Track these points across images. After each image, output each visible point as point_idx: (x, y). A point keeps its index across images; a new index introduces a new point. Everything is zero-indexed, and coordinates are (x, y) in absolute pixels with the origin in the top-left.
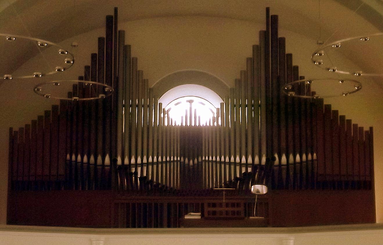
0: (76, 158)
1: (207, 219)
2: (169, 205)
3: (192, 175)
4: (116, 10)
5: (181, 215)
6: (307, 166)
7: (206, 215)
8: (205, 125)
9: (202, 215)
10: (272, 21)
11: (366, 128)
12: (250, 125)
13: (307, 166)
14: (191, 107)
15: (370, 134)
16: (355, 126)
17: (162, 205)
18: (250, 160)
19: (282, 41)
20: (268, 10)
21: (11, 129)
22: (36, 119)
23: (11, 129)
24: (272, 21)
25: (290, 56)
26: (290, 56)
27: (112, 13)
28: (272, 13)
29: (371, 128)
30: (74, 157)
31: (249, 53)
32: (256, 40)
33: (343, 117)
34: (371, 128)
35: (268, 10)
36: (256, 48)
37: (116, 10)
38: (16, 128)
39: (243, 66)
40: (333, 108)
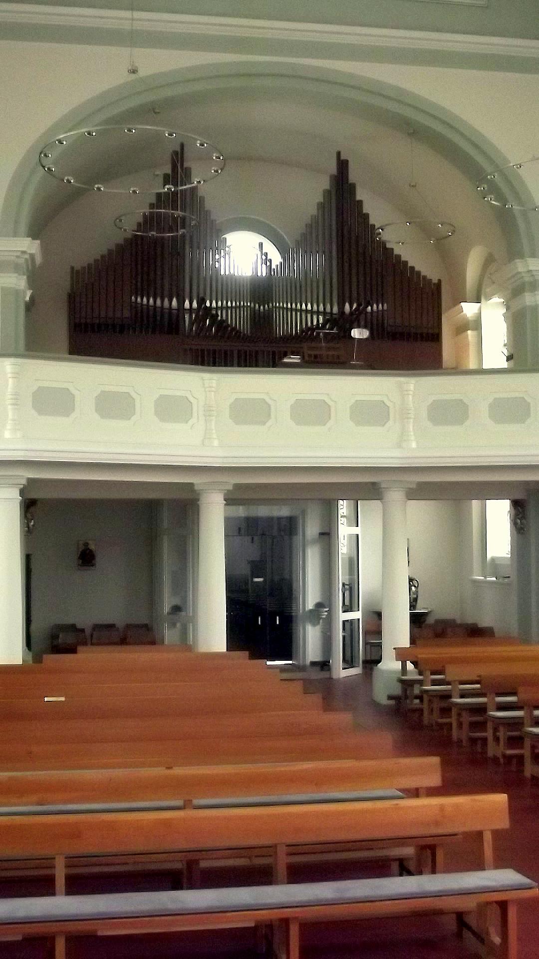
0: (148, 301)
1: (307, 362)
2: (239, 351)
3: (262, 322)
4: (182, 146)
5: (281, 358)
6: (377, 316)
7: (307, 358)
8: (263, 272)
9: (303, 358)
10: (343, 165)
11: (435, 281)
12: (321, 274)
13: (377, 316)
14: (243, 255)
15: (439, 285)
16: (425, 277)
17: (232, 351)
18: (321, 308)
19: (352, 188)
20: (339, 154)
21: (72, 268)
22: (99, 258)
23: (72, 268)
24: (343, 165)
25: (360, 202)
26: (360, 202)
27: (178, 149)
28: (342, 158)
29: (440, 281)
30: (139, 300)
31: (320, 199)
32: (325, 183)
33: (412, 268)
34: (440, 281)
35: (339, 154)
36: (327, 193)
37: (182, 146)
38: (78, 266)
39: (313, 210)
40: (403, 259)
